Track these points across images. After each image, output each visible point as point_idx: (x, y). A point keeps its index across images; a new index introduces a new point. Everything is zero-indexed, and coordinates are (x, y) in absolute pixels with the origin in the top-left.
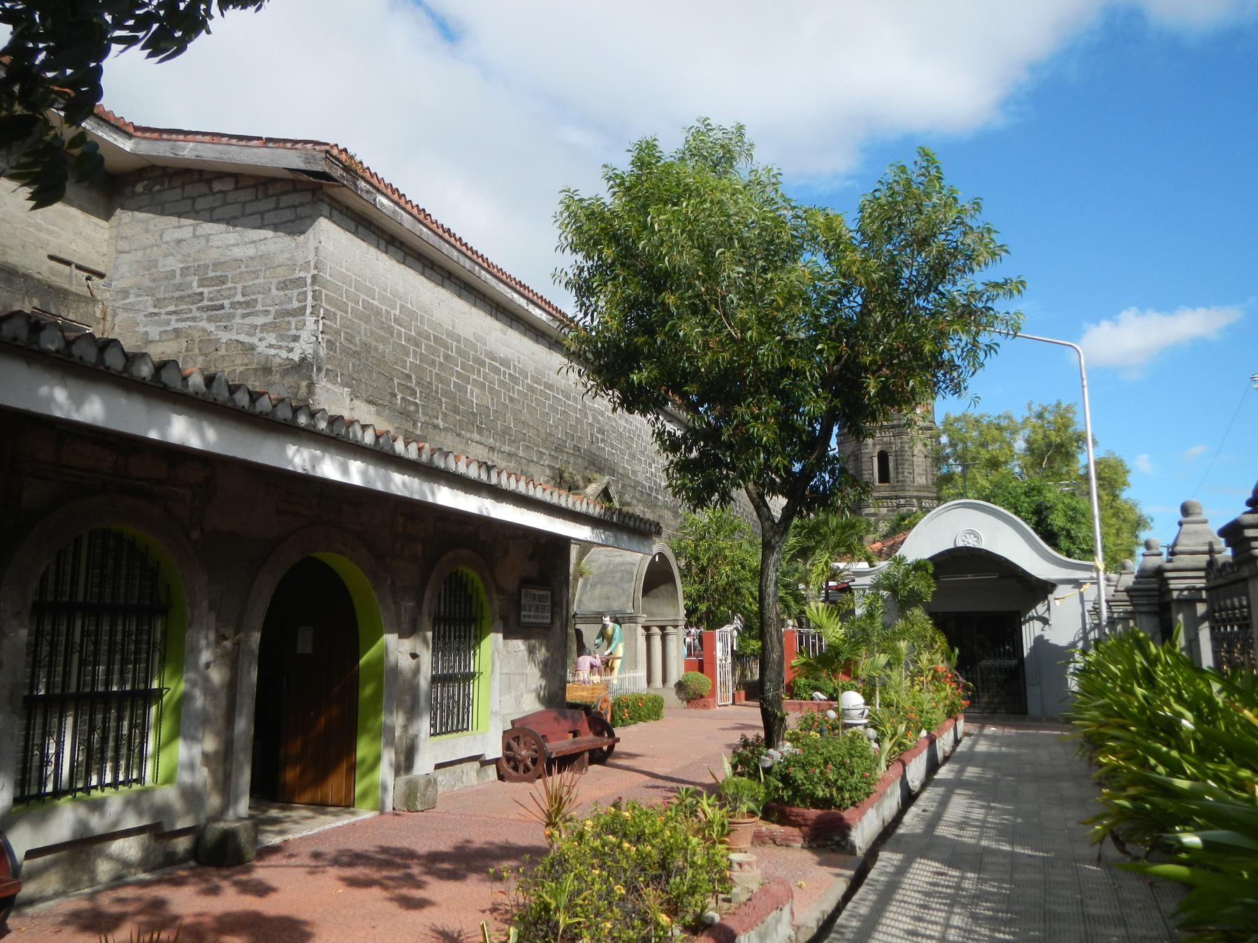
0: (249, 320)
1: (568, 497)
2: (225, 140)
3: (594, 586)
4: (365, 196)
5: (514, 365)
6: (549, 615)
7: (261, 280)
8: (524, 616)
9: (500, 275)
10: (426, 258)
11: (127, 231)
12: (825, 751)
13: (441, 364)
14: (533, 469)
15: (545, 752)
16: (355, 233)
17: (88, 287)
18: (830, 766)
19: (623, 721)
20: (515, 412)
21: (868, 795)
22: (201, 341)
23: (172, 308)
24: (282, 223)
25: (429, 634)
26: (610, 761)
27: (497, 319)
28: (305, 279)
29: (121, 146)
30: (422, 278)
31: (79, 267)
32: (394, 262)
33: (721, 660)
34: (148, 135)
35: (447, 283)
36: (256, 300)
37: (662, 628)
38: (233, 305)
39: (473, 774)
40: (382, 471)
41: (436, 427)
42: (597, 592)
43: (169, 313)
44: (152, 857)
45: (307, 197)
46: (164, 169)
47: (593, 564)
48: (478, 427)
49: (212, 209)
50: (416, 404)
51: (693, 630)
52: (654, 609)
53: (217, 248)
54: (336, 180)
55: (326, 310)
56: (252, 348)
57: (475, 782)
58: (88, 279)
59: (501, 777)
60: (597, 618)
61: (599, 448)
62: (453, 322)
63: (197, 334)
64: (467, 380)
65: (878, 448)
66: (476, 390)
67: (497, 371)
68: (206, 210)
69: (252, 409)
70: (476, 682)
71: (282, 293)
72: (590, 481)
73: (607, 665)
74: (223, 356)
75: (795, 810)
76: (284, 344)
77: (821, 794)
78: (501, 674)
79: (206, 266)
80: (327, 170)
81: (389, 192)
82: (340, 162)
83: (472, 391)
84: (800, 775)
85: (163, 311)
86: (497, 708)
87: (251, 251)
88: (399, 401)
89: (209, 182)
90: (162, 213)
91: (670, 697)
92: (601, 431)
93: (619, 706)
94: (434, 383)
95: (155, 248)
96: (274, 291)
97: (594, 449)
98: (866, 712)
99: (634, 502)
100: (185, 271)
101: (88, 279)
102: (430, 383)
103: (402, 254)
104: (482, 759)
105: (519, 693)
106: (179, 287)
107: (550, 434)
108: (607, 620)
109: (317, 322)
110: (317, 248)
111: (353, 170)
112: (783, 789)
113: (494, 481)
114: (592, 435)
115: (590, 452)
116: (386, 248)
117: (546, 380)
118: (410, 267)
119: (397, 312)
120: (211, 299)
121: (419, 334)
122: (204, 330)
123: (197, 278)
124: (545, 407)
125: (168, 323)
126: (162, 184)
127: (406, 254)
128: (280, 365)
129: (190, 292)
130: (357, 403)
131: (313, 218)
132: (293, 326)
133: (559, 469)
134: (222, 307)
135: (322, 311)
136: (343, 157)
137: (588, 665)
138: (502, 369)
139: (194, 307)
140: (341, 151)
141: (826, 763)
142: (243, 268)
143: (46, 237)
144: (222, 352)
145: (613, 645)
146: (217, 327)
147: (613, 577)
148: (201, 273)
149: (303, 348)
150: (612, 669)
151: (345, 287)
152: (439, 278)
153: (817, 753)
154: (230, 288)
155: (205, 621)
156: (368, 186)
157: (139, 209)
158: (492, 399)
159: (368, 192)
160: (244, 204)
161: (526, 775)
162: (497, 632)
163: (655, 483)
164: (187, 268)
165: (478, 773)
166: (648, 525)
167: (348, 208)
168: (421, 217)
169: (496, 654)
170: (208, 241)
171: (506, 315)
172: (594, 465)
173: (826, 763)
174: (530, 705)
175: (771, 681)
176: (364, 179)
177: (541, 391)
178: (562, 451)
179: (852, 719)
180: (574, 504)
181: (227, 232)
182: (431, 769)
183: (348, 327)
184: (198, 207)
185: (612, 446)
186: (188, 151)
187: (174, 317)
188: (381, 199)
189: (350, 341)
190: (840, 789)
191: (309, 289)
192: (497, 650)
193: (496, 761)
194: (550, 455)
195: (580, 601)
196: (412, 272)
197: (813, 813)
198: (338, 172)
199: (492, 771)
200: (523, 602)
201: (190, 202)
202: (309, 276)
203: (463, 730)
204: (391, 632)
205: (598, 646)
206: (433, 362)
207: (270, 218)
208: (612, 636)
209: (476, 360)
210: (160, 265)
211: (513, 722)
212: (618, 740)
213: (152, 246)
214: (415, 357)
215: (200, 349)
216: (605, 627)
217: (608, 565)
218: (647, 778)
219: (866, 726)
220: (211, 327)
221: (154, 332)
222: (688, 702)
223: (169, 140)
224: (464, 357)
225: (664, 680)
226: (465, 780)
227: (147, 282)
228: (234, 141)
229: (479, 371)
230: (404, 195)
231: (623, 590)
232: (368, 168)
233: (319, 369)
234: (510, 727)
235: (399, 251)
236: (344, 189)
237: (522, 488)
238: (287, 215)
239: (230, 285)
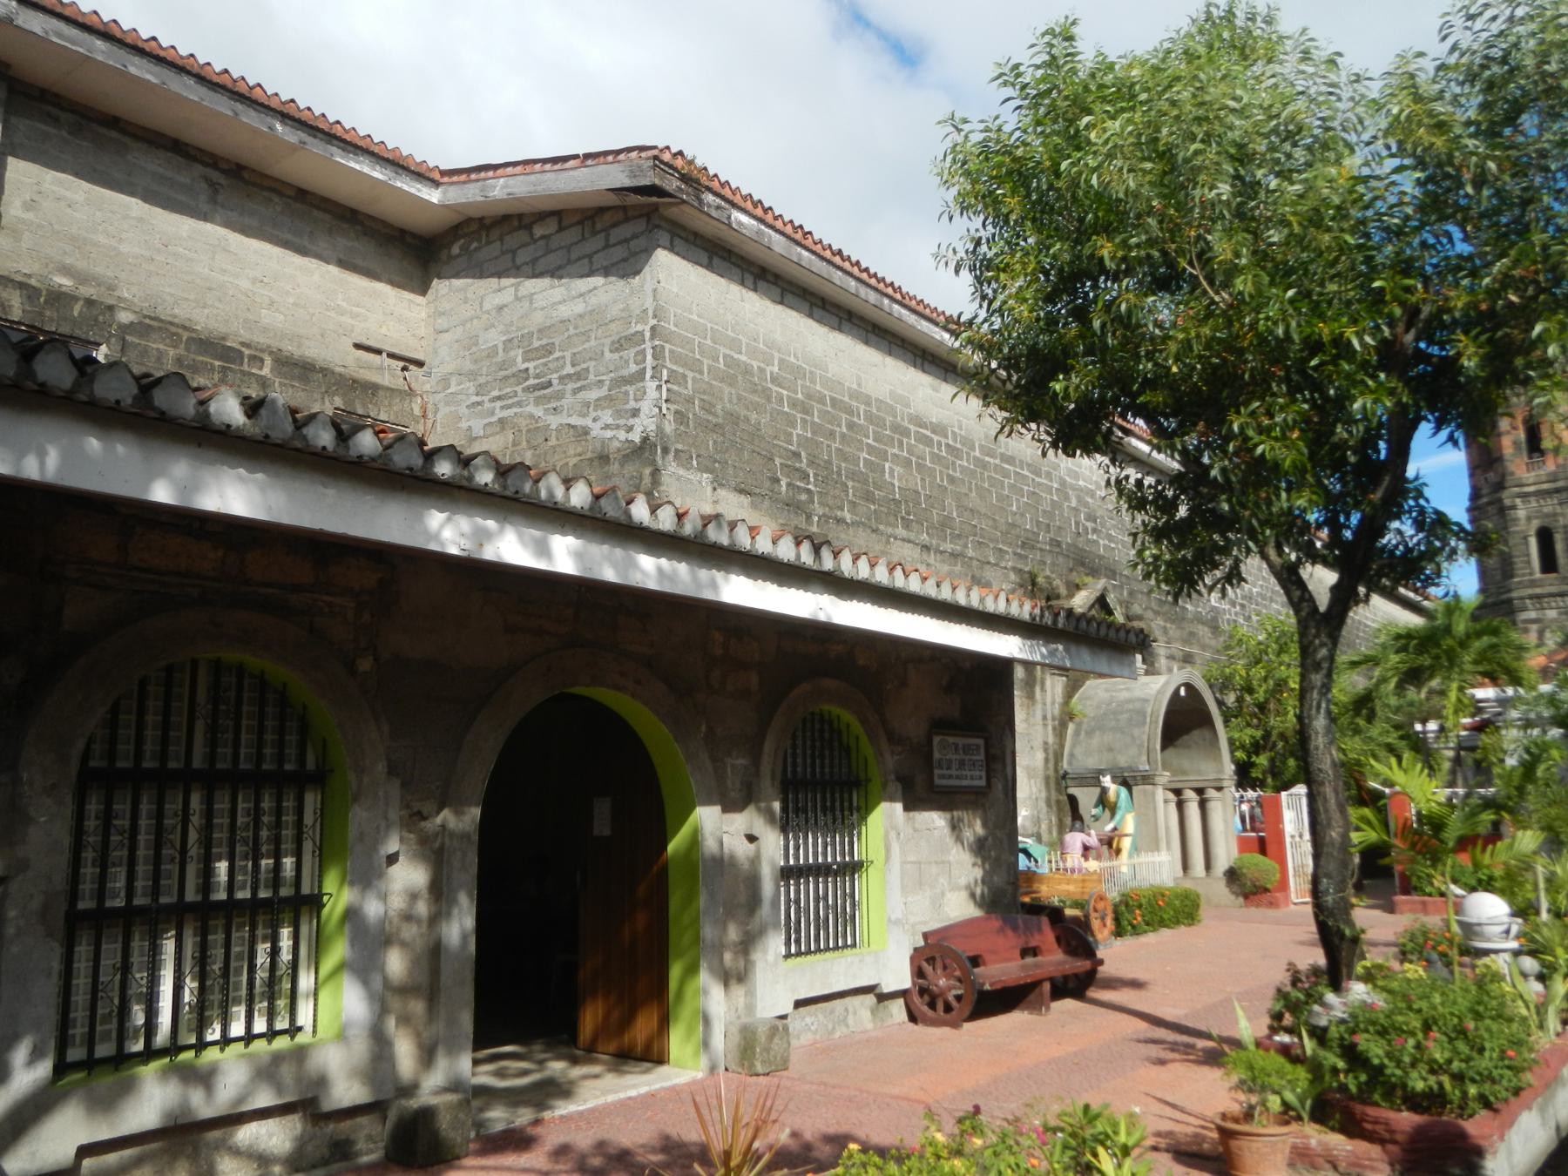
0: (582, 395)
1: (969, 589)
2: (538, 166)
3: (1090, 733)
4: (714, 213)
5: (953, 432)
6: (983, 774)
7: (593, 343)
8: (942, 777)
9: (920, 308)
10: (812, 294)
11: (445, 305)
12: (1424, 1005)
13: (843, 436)
14: (989, 574)
15: (973, 983)
16: (709, 267)
17: (405, 379)
18: (1435, 1034)
19: (1134, 927)
20: (958, 498)
21: (1517, 1092)
22: (529, 431)
23: (496, 393)
24: (613, 265)
25: (777, 806)
26: (1093, 993)
27: (924, 371)
28: (642, 333)
29: (427, 197)
30: (810, 322)
31: (391, 356)
32: (768, 303)
33: (1293, 837)
34: (455, 178)
35: (846, 325)
36: (587, 370)
37: (1200, 791)
38: (561, 378)
39: (866, 1015)
40: (618, 552)
41: (840, 521)
42: (1096, 740)
43: (493, 400)
44: (309, 1148)
45: (640, 225)
46: (481, 219)
47: (1088, 703)
48: (902, 518)
49: (534, 261)
50: (809, 491)
51: (1250, 794)
52: (1186, 764)
53: (542, 309)
54: (670, 195)
55: (671, 372)
56: (585, 432)
57: (870, 1026)
58: (404, 369)
59: (913, 1018)
60: (1093, 779)
61: (1089, 541)
62: (859, 378)
63: (524, 423)
64: (884, 456)
65: (1536, 524)
66: (898, 470)
67: (928, 442)
68: (527, 263)
69: (341, 452)
70: (864, 875)
71: (616, 356)
72: (1078, 587)
73: (1110, 844)
74: (553, 447)
75: (1371, 1111)
76: (622, 422)
77: (1420, 1086)
78: (903, 863)
79: (531, 334)
80: (657, 182)
81: (749, 206)
82: (675, 169)
83: (892, 471)
84: (1375, 1050)
85: (486, 398)
86: (897, 914)
87: (579, 307)
88: (784, 488)
89: (529, 228)
90: (481, 277)
91: (1216, 891)
92: (1091, 518)
93: (1127, 905)
94: (835, 462)
95: (475, 321)
96: (608, 355)
97: (1081, 542)
98: (1515, 929)
99: (1149, 614)
100: (509, 345)
101: (404, 369)
102: (829, 462)
103: (779, 290)
104: (878, 991)
105: (938, 891)
106: (502, 366)
107: (1013, 525)
108: (1107, 781)
109: (659, 387)
110: (655, 290)
111: (695, 179)
112: (1347, 1072)
113: (828, 564)
114: (1077, 524)
115: (1076, 547)
116: (755, 283)
117: (1003, 450)
118: (792, 308)
119: (776, 369)
120: (537, 376)
121: (809, 396)
122: (531, 416)
123: (521, 351)
124: (1003, 487)
125: (493, 413)
126: (479, 241)
127: (783, 290)
128: (619, 450)
129: (515, 369)
130: (722, 493)
131: (648, 252)
132: (632, 397)
133: (1030, 573)
134: (550, 384)
135: (665, 372)
136: (679, 163)
137: (1079, 846)
138: (936, 438)
139: (519, 389)
140: (675, 155)
141: (1427, 1027)
142: (572, 331)
143: (349, 321)
144: (553, 442)
145: (1118, 817)
146: (545, 410)
147: (1118, 720)
148: (526, 343)
149: (645, 424)
150: (1118, 851)
151: (697, 339)
152: (835, 320)
153: (1410, 1008)
154: (558, 359)
155: (381, 794)
156: (718, 200)
157: (457, 276)
158: (922, 479)
159: (718, 207)
160: (569, 248)
161: (948, 1016)
162: (892, 799)
164: (510, 341)
165: (874, 1012)
166: (1122, 634)
167: (696, 234)
168: (799, 236)
169: (893, 834)
170: (531, 303)
171: (937, 366)
172: (1083, 564)
173: (1427, 1027)
174: (959, 908)
175: (1328, 876)
176: (709, 189)
177: (996, 465)
178: (1033, 547)
179: (1489, 940)
180: (982, 600)
181: (553, 287)
182: (787, 1008)
183: (704, 393)
184: (519, 261)
185: (1110, 538)
186: (499, 189)
187: (499, 404)
188: (738, 217)
189: (710, 413)
190: (1459, 1078)
191: (648, 345)
192: (894, 827)
193: (903, 994)
194: (1015, 554)
195: (1072, 755)
196: (794, 314)
197: (1406, 1120)
198: (672, 184)
199: (898, 1009)
200: (937, 755)
201: (509, 256)
202: (647, 328)
203: (845, 946)
204: (708, 802)
205: (1096, 818)
206: (832, 434)
207: (600, 260)
208: (1116, 803)
209: (896, 428)
210: (481, 341)
211: (926, 936)
212: (1101, 962)
213: (472, 319)
214: (804, 428)
215: (528, 442)
216: (1104, 791)
218: (1142, 1025)
219: (1517, 954)
220: (538, 412)
221: (477, 426)
222: (1246, 897)
223: (477, 180)
224: (877, 425)
225: (1208, 866)
226: (851, 1020)
228: (548, 166)
229: (901, 443)
230: (770, 208)
231: (1133, 736)
232: (716, 175)
233: (665, 450)
234: (922, 943)
235: (773, 287)
236: (685, 207)
237: (881, 576)
238: (618, 253)
239: (557, 354)
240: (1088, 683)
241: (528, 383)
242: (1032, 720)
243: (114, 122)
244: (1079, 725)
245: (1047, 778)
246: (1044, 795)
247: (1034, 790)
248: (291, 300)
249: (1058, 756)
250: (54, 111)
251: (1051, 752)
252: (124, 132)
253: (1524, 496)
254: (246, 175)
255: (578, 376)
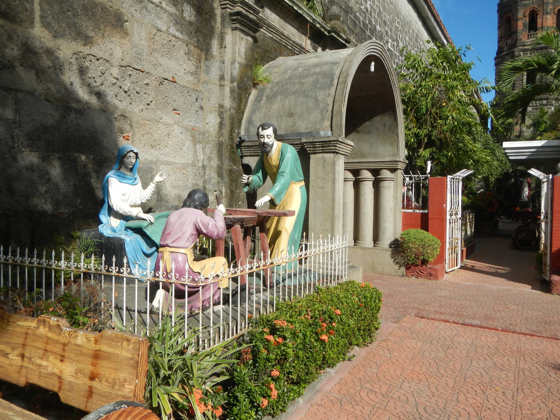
37: (376, 172)
42: (276, 106)
47: (275, 70)
137: (190, 230)
147: (303, 84)
163: (370, 22)
208: (278, 167)
217: (297, 69)
222: (408, 268)
225: (376, 238)
231: (316, 100)
240: (280, 58)
242: (203, 76)
244: (263, 90)
245: (220, 145)
246: (215, 163)
247: (201, 157)
249: (236, 121)
251: (226, 116)
253: (525, 51)
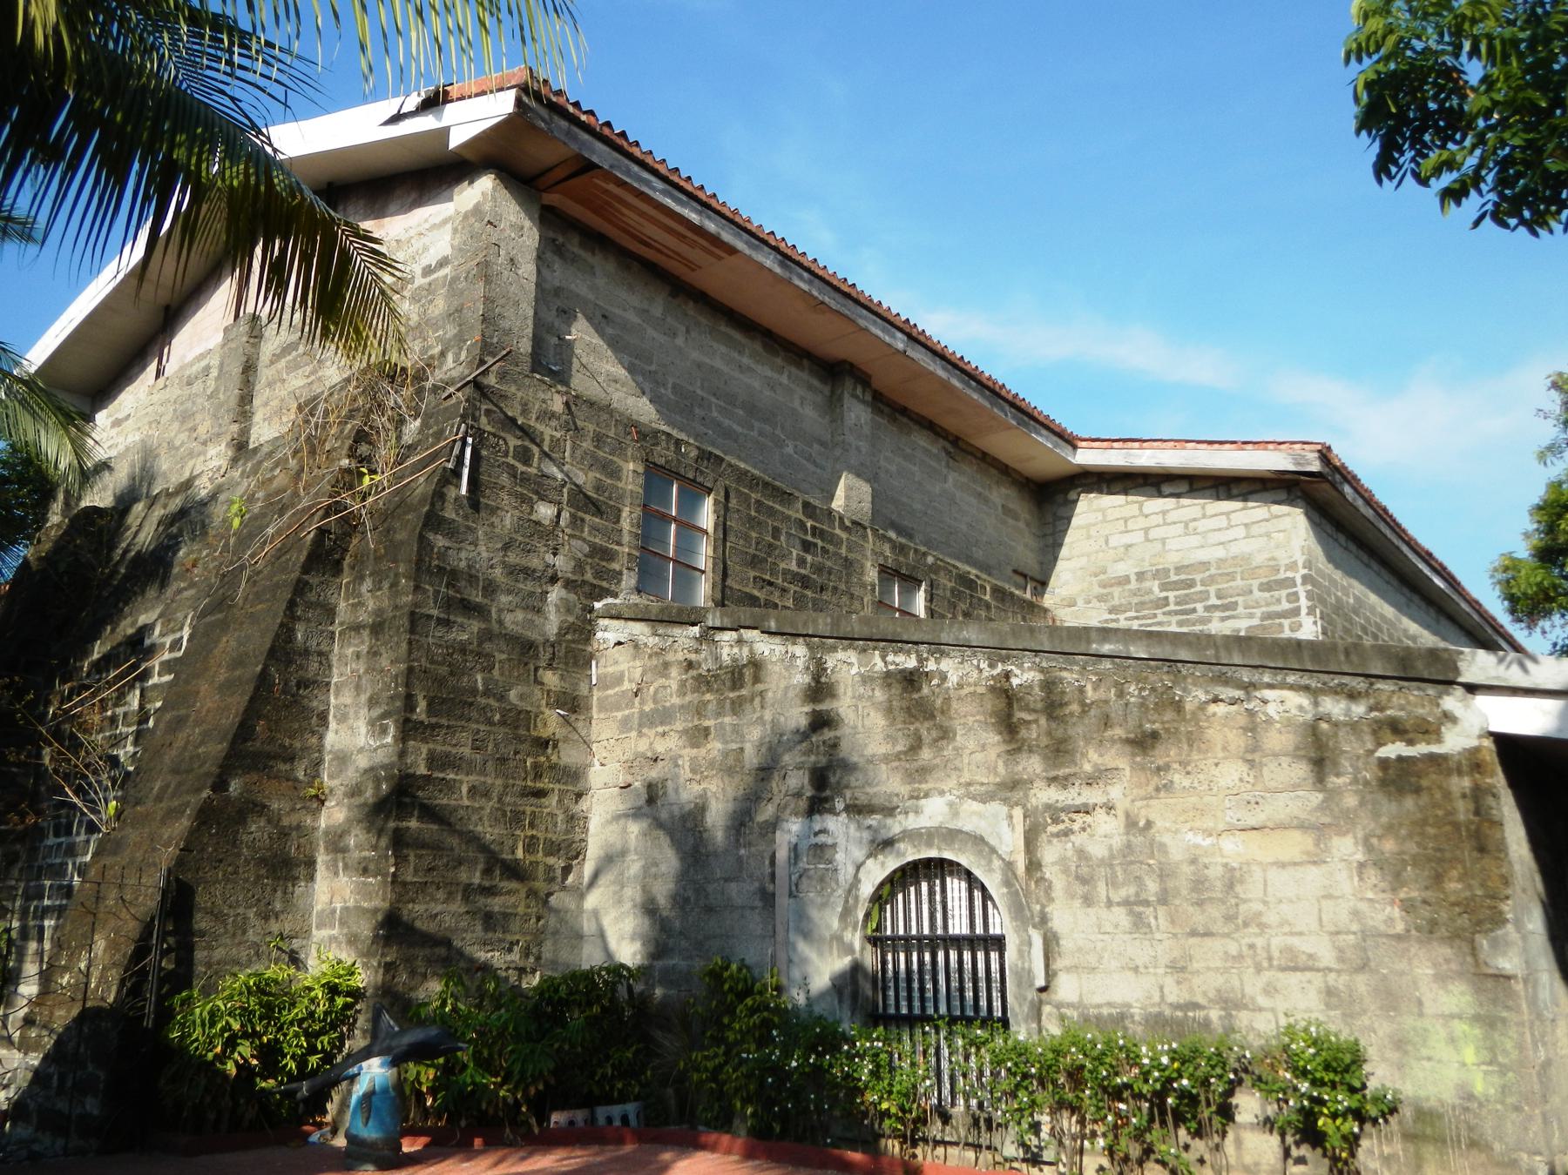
23: (1133, 614)
38: (1207, 609)
71: (1267, 595)
85: (1122, 617)
170: (1164, 544)
213: (1097, 552)
227: (1097, 590)
239: (1199, 588)
241: (1168, 609)
243: (904, 411)
248: (985, 539)
250: (882, 407)
252: (911, 419)
254: (960, 443)
255: (1225, 608)
